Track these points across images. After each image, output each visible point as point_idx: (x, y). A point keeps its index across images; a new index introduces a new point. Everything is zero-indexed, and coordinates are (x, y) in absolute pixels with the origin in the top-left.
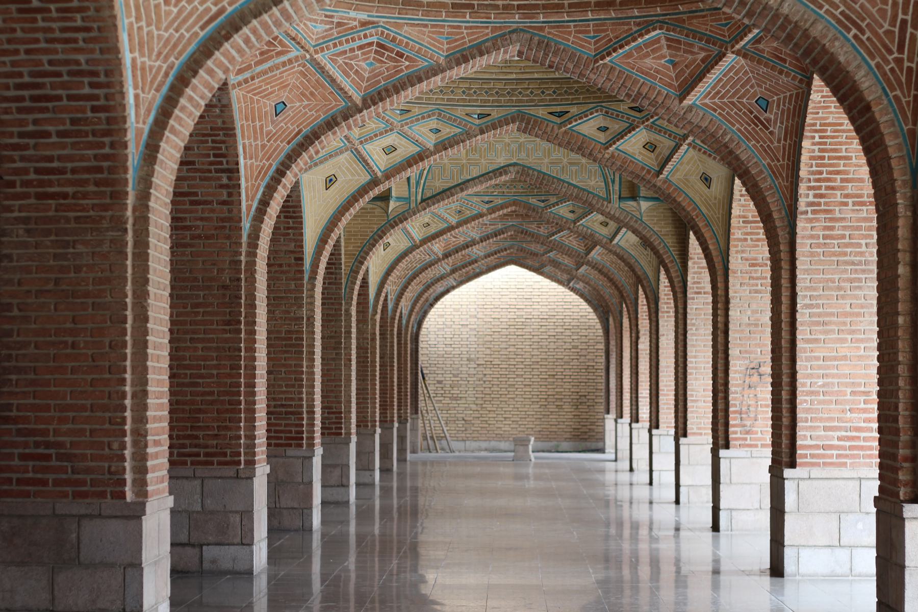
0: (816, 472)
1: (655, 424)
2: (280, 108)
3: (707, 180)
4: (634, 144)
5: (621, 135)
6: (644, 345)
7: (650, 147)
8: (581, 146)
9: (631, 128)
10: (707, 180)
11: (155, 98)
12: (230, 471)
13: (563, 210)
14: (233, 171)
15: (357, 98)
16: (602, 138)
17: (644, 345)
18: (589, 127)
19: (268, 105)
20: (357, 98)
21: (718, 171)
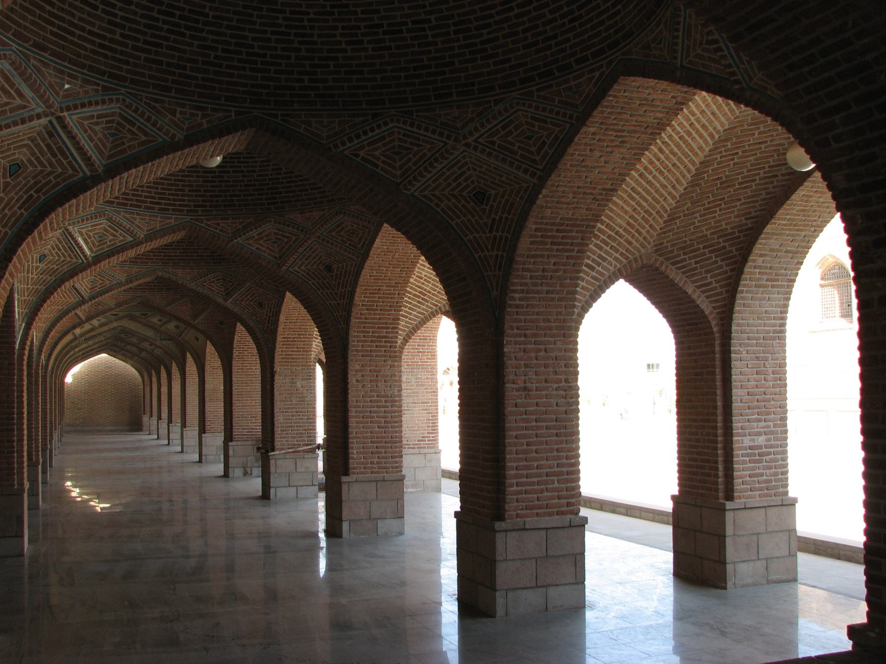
0: (239, 443)
1: (170, 421)
3: (197, 339)
4: (171, 326)
5: (166, 323)
6: (164, 389)
7: (177, 327)
8: (152, 327)
9: (170, 321)
10: (197, 339)
11: (41, 335)
13: (134, 340)
15: (83, 318)
16: (159, 323)
17: (164, 389)
18: (155, 320)
20: (83, 318)
21: (201, 336)
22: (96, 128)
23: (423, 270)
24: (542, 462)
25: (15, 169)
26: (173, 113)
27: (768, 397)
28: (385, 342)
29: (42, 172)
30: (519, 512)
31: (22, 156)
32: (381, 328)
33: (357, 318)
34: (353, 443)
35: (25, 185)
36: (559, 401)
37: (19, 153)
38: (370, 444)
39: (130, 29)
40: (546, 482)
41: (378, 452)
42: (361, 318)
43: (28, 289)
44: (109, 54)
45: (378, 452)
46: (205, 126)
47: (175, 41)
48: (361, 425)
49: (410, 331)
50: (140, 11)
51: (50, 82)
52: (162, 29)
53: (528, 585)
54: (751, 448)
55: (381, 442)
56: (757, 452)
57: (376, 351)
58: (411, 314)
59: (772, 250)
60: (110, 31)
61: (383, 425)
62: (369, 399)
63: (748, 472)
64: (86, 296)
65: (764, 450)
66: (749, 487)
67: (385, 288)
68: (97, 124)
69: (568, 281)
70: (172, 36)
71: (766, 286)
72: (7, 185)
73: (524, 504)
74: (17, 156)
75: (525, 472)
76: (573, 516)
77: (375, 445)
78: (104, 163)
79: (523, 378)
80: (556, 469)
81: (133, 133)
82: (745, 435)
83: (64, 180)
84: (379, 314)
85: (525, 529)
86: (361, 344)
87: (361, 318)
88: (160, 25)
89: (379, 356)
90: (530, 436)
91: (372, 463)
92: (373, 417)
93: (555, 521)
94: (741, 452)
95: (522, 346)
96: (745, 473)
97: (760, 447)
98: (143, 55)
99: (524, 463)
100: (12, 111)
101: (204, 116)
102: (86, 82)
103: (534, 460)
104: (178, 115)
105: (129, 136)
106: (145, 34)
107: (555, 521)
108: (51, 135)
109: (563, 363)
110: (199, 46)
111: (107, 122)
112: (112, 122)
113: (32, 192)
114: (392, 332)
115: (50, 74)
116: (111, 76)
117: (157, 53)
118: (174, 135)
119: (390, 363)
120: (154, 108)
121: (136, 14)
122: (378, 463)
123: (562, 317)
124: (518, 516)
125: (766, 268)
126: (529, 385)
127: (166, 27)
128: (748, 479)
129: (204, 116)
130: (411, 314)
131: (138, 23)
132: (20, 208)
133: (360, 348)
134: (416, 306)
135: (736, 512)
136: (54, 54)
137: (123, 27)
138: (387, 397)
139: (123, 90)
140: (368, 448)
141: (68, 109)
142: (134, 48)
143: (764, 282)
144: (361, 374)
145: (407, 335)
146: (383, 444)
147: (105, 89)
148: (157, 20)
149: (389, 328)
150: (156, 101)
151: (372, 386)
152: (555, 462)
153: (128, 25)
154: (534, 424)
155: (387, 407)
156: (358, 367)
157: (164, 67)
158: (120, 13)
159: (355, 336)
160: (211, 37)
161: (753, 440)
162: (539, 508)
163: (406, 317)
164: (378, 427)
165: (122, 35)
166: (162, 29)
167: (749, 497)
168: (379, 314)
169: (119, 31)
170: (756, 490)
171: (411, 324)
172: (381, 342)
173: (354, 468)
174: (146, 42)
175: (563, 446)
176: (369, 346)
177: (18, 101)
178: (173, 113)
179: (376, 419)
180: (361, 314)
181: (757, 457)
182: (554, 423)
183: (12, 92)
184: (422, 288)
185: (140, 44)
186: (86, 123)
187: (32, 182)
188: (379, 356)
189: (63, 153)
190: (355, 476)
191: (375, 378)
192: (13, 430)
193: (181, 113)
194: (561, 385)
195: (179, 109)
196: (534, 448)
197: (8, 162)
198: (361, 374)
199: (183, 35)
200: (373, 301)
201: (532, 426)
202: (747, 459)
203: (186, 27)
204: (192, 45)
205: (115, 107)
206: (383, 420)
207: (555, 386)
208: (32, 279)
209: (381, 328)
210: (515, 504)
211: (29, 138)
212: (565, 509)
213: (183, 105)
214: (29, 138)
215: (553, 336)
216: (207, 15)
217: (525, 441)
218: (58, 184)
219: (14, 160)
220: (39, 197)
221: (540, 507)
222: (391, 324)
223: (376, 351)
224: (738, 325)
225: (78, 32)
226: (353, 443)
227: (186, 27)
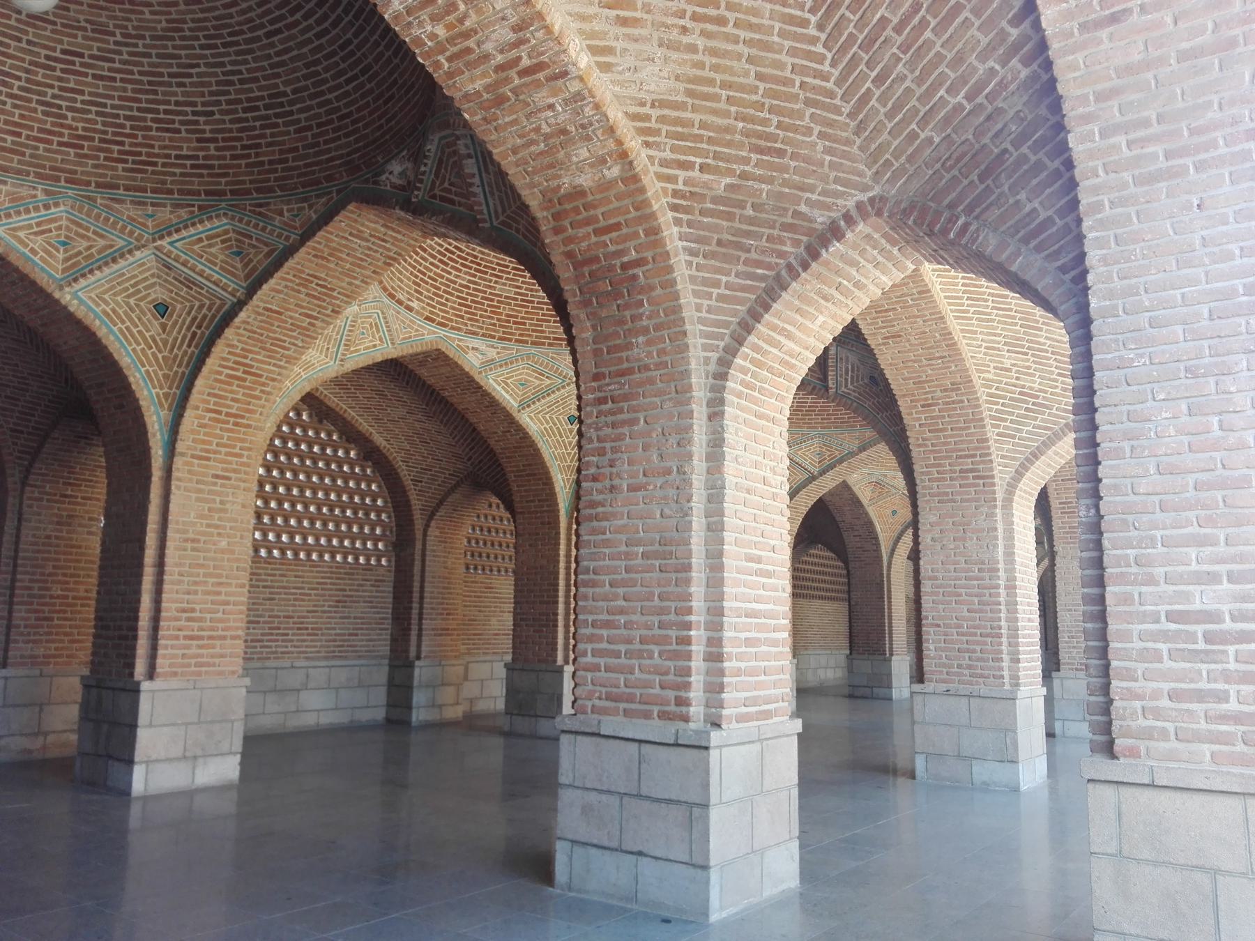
2: (894, 513)
12: (882, 657)
14: (876, 538)
19: (889, 512)
22: (213, 250)
23: (1003, 356)
24: (634, 618)
25: (162, 309)
26: (281, 214)
27: (1236, 473)
28: (974, 478)
29: (192, 307)
30: (597, 702)
31: (159, 294)
32: (961, 457)
33: (920, 446)
34: (929, 633)
35: (183, 323)
36: (667, 511)
37: (155, 292)
38: (955, 637)
39: (224, 140)
40: (639, 655)
41: (968, 651)
42: (926, 446)
43: (569, 454)
44: (205, 172)
45: (968, 651)
46: (314, 217)
47: (272, 135)
48: (941, 607)
49: (1027, 459)
50: (227, 118)
51: (129, 217)
52: (254, 128)
53: (606, 843)
54: (1171, 617)
55: (975, 635)
56: (1199, 629)
57: (959, 493)
58: (1020, 431)
59: (1129, 69)
60: (202, 149)
61: (976, 607)
62: (952, 567)
63: (1166, 686)
64: (816, 471)
65: (1228, 625)
66: (1170, 726)
67: (939, 394)
68: (210, 246)
69: (659, 291)
70: (268, 131)
71: (1170, 174)
72: (164, 327)
73: (604, 690)
74: (153, 296)
75: (605, 632)
76: (681, 725)
77: (964, 638)
78: (244, 285)
79: (607, 470)
80: (657, 632)
81: (254, 246)
82: (1151, 581)
83: (218, 311)
84: (951, 436)
85: (599, 735)
86: (935, 484)
87: (926, 446)
88: (251, 124)
89: (967, 501)
90: (614, 571)
91: (959, 666)
92: (960, 595)
93: (653, 729)
94: (1137, 628)
95: (610, 419)
96: (1154, 685)
97: (1211, 617)
98: (243, 162)
99: (604, 617)
100: (99, 252)
101: (310, 207)
102: (177, 206)
103: (622, 611)
104: (286, 214)
105: (253, 251)
106: (240, 139)
107: (653, 729)
108: (170, 269)
109: (673, 440)
110: (296, 131)
111: (223, 242)
112: (230, 240)
113: (194, 328)
114: (983, 462)
115: (128, 209)
116: (207, 193)
117: (257, 155)
118: (287, 238)
119: (985, 510)
120: (260, 214)
121: (224, 122)
122: (969, 667)
123: (668, 358)
124: (594, 710)
125: (1146, 123)
126: (616, 482)
127: (258, 124)
128: (1165, 702)
129: (310, 207)
130: (1020, 431)
131: (231, 131)
132: (189, 346)
133: (935, 490)
134: (1026, 417)
135: (1126, 792)
136: (127, 188)
137: (215, 140)
138: (983, 563)
139: (223, 204)
140: (952, 642)
141: (161, 238)
142: (233, 157)
143: (1162, 163)
144: (938, 528)
145: (1022, 465)
146: (979, 638)
147: (200, 208)
148: (247, 120)
149: (974, 456)
150: (260, 205)
151: (957, 547)
152: (656, 619)
153: (220, 136)
154: (623, 548)
155: (982, 579)
156: (933, 519)
157: (267, 167)
158: (208, 128)
159: (922, 473)
160: (302, 116)
161: (1187, 597)
162: (627, 701)
163: (1013, 437)
164: (969, 611)
165: (217, 149)
166: (254, 128)
167: (1171, 756)
168: (951, 436)
169: (212, 146)
170: (1198, 738)
171: (1026, 447)
172: (967, 478)
173: (933, 672)
174: (244, 147)
175: (670, 589)
176: (949, 486)
177: (101, 243)
178: (281, 214)
179: (964, 597)
180: (924, 439)
181: (1201, 645)
182: (657, 547)
183: (90, 234)
184: (1023, 387)
185: (239, 152)
186: (196, 247)
187: (189, 319)
188: (967, 501)
189: (193, 283)
190: (933, 684)
191: (961, 534)
192: (557, 602)
193: (288, 211)
194: (670, 478)
195: (285, 208)
196: (621, 591)
197: (150, 303)
198: (938, 528)
199: (276, 125)
200: (932, 418)
201: (619, 553)
202: (1163, 647)
203: (277, 116)
204: (288, 133)
205: (220, 224)
206: (976, 600)
207: (659, 482)
208: (570, 443)
209: (961, 457)
210: (590, 687)
211: (153, 276)
212: (672, 708)
213: (288, 203)
214: (153, 276)
215: (660, 393)
216: (285, 94)
217: (607, 578)
218: (214, 316)
219: (154, 300)
220: (203, 333)
221: (630, 699)
222: (977, 449)
223: (959, 493)
224: (1111, 295)
225: (160, 161)
226: (929, 633)
227: (277, 116)
